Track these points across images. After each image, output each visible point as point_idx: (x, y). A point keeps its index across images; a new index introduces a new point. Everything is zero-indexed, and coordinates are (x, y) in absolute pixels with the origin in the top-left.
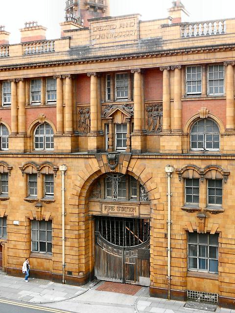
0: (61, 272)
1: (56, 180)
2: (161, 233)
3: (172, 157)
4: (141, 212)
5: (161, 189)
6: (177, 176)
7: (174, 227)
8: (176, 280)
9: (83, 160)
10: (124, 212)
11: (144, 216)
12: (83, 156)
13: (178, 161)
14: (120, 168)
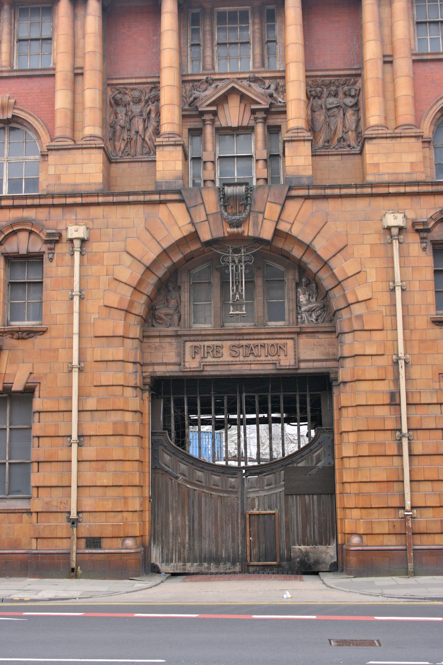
0: (61, 546)
1: (52, 270)
2: (378, 392)
3: (402, 190)
4: (306, 354)
5: (372, 275)
6: (416, 237)
7: (416, 372)
8: (426, 519)
9: (141, 208)
10: (251, 358)
11: (310, 365)
12: (141, 198)
13: (415, 199)
14: (256, 224)
